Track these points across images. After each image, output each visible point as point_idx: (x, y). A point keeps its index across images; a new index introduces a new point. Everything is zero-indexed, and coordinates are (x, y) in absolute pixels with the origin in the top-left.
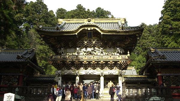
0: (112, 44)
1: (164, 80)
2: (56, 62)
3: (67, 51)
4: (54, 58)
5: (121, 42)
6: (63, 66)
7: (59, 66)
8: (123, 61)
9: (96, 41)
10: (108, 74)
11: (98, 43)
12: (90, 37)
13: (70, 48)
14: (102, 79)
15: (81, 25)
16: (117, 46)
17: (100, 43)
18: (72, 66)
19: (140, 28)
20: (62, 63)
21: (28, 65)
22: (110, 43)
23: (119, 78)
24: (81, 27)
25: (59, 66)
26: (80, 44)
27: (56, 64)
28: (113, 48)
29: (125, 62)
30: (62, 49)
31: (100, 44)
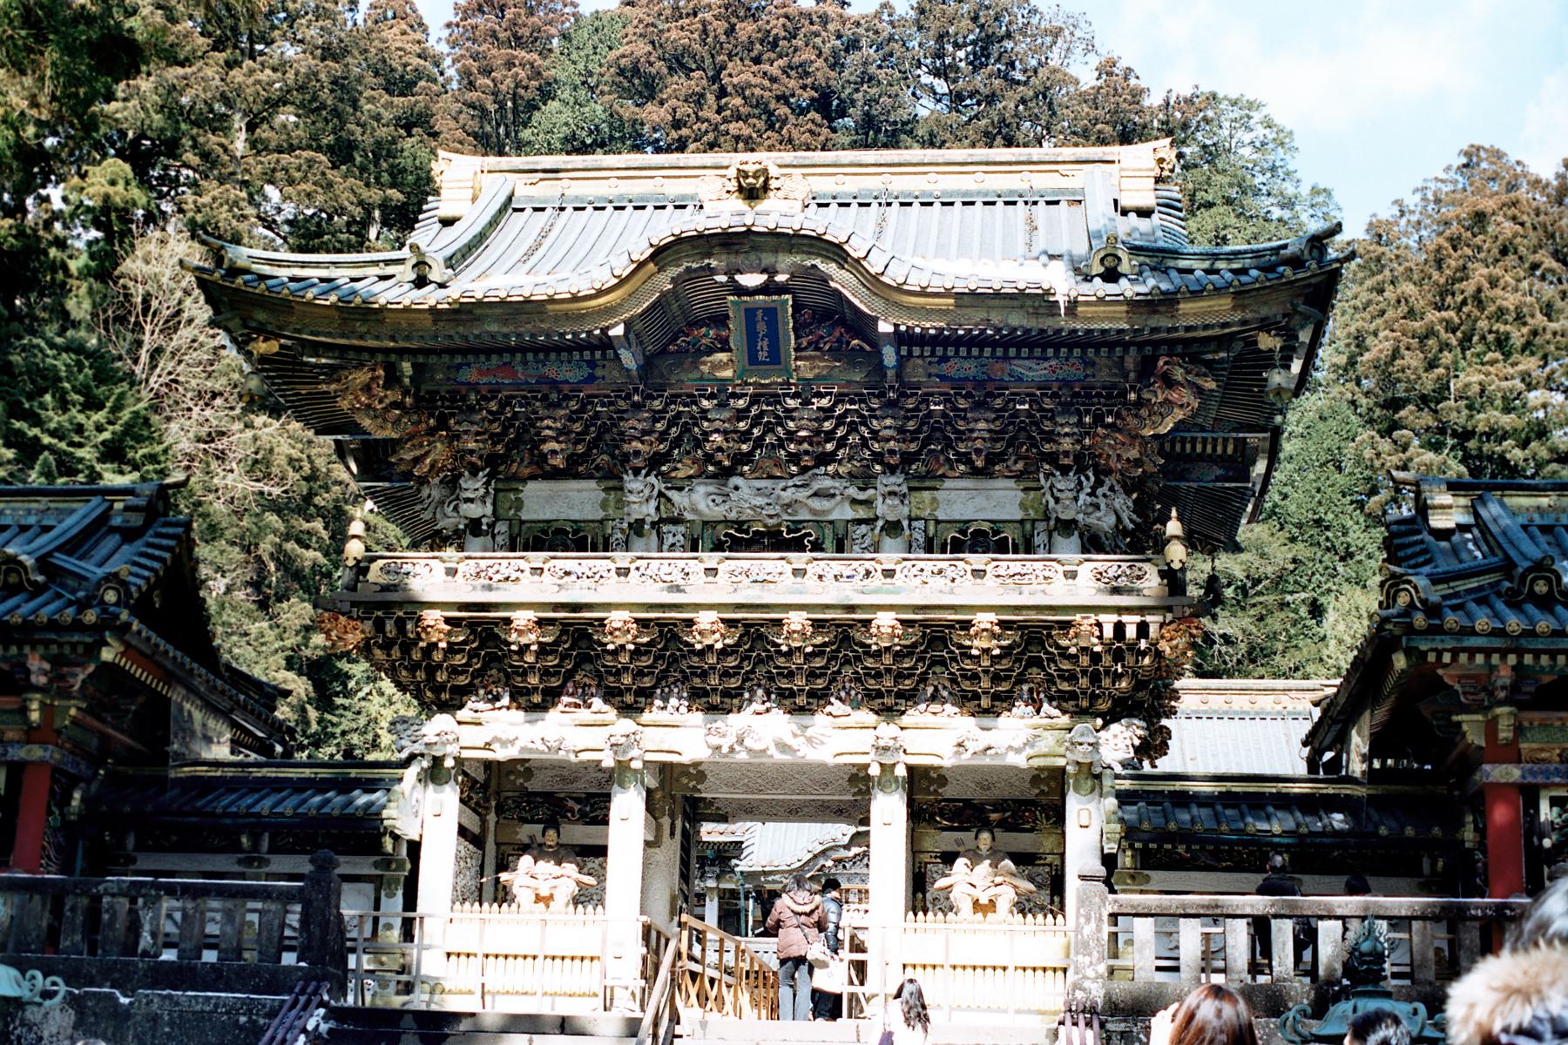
0: (995, 436)
2: (400, 624)
3: (519, 505)
4: (385, 588)
5: (1099, 419)
8: (1109, 620)
9: (825, 402)
11: (853, 428)
12: (762, 356)
15: (667, 226)
21: (107, 655)
24: (660, 255)
25: (431, 670)
28: (1018, 477)
29: (1131, 632)
30: (473, 486)
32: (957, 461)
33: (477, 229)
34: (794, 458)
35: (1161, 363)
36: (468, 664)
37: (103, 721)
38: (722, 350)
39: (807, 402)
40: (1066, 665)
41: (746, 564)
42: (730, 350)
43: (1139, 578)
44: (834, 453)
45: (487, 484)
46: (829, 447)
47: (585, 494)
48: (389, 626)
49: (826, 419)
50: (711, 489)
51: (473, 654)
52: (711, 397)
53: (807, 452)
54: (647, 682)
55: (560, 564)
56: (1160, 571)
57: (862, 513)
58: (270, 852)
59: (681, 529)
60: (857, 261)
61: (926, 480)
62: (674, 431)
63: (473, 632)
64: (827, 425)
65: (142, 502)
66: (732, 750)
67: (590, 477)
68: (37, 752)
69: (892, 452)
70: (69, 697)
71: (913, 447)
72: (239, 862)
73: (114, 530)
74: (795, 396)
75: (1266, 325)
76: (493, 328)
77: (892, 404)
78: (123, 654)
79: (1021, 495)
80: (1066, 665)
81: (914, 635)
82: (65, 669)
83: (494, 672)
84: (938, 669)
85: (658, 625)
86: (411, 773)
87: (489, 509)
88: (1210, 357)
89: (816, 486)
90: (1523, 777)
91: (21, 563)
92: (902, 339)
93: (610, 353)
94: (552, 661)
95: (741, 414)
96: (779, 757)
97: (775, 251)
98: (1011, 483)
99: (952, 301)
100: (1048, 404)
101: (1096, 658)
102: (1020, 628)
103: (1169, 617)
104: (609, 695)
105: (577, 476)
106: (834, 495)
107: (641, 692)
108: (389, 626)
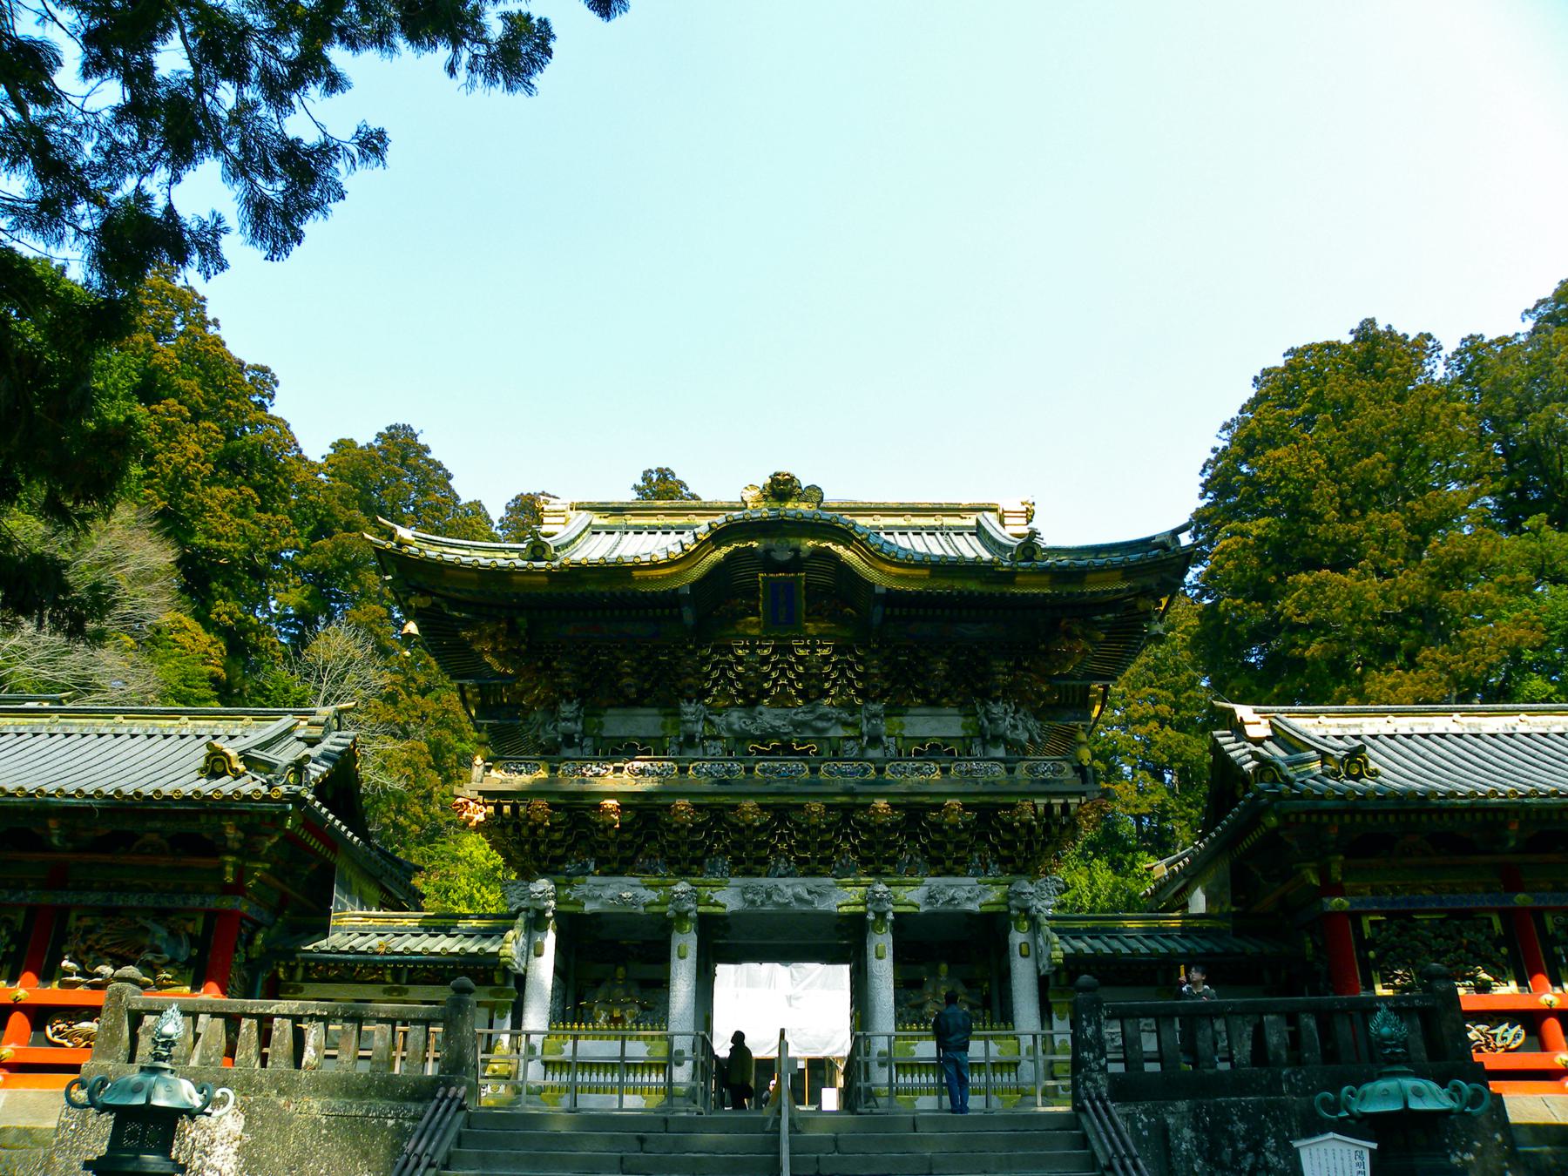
0: (946, 678)
1: (1371, 944)
2: (515, 808)
3: (601, 726)
5: (1018, 666)
6: (571, 848)
7: (535, 845)
8: (1041, 802)
9: (826, 652)
10: (922, 910)
13: (625, 706)
14: (882, 943)
16: (986, 695)
17: (860, 669)
18: (639, 841)
19: (1163, 546)
20: (560, 816)
22: (940, 667)
23: (1018, 938)
24: (718, 536)
25: (535, 845)
26: (707, 676)
27: (517, 828)
28: (960, 706)
29: (1057, 810)
30: (567, 709)
31: (860, 676)
32: (917, 696)
33: (572, 536)
34: (800, 694)
35: (1063, 624)
36: (563, 840)
37: (281, 880)
38: (752, 615)
39: (813, 651)
40: (1008, 837)
41: (777, 765)
42: (757, 614)
43: (1059, 772)
44: (828, 690)
45: (578, 709)
46: (827, 685)
47: (650, 719)
48: (507, 809)
49: (826, 665)
50: (742, 714)
51: (568, 832)
52: (744, 647)
53: (814, 686)
54: (699, 853)
55: (637, 764)
56: (1074, 768)
57: (851, 732)
58: (408, 983)
59: (719, 744)
60: (860, 542)
61: (894, 710)
62: (715, 674)
63: (569, 816)
64: (827, 669)
65: (321, 719)
66: (763, 903)
67: (652, 706)
68: (228, 903)
69: (875, 687)
70: (258, 860)
71: (886, 685)
72: (385, 991)
73: (299, 739)
74: (804, 647)
75: (1145, 592)
76: (591, 587)
77: (874, 652)
78: (303, 826)
79: (961, 720)
80: (1008, 837)
81: (899, 816)
82: (256, 838)
83: (583, 847)
84: (912, 843)
85: (712, 811)
86: (520, 920)
87: (579, 727)
88: (1099, 618)
89: (820, 711)
90: (1351, 906)
91: (225, 754)
92: (892, 597)
93: (676, 611)
94: (628, 836)
95: (765, 660)
96: (795, 906)
97: (801, 535)
98: (955, 711)
99: (926, 572)
100: (982, 653)
101: (1031, 829)
102: (973, 811)
103: (1084, 799)
104: (671, 862)
105: (643, 706)
106: (830, 719)
107: (694, 861)
108: (507, 809)
